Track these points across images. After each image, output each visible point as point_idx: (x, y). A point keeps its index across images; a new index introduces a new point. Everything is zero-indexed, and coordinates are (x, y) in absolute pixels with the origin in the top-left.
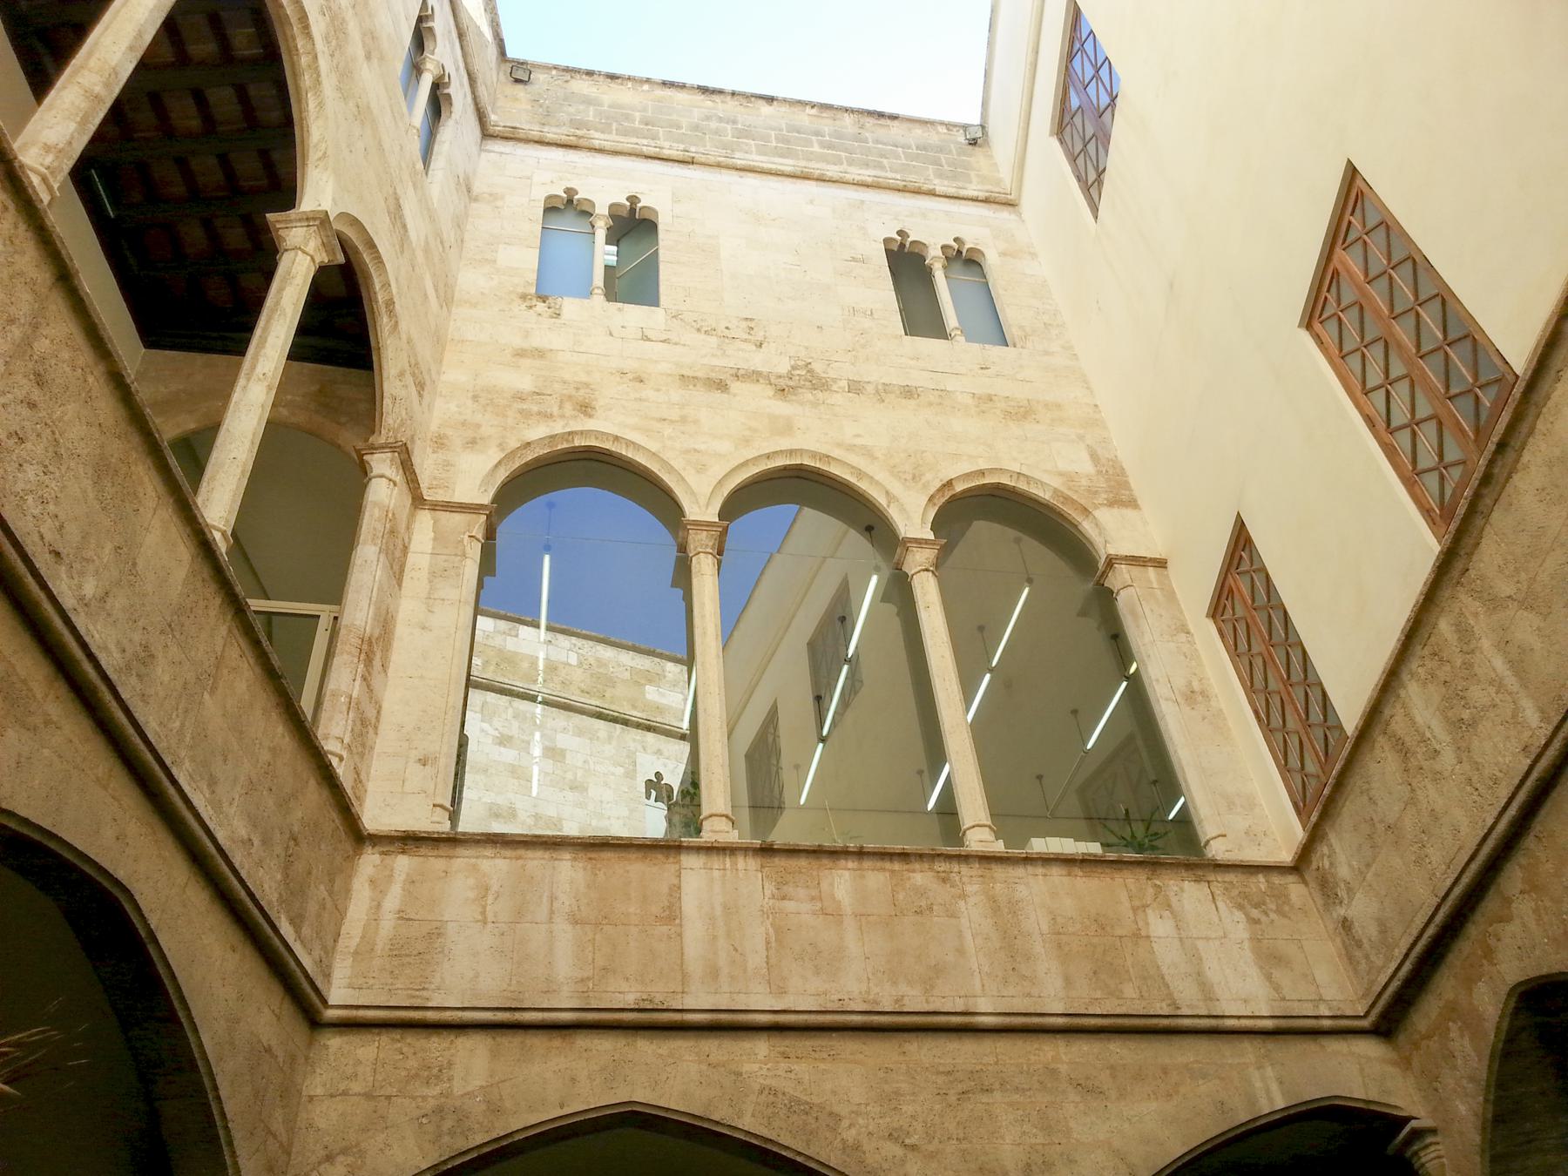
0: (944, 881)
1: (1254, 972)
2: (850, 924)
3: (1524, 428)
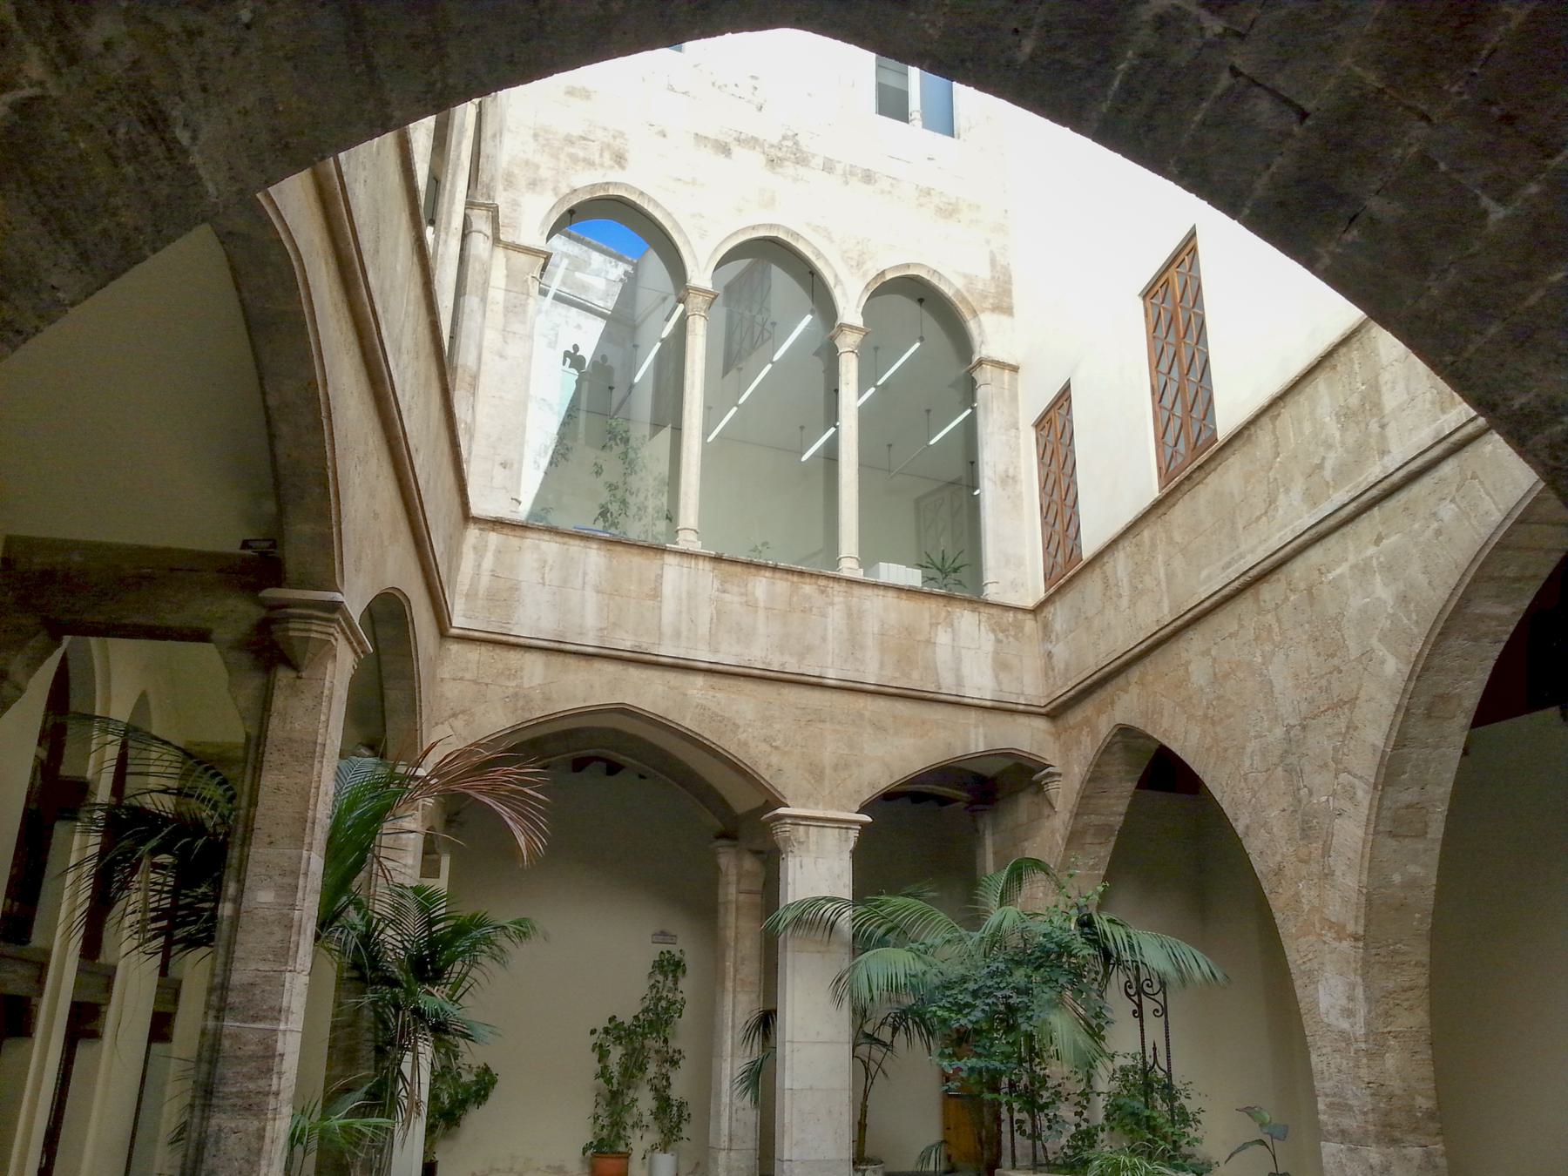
0: (823, 592)
1: (989, 673)
2: (761, 613)
3: (1213, 465)
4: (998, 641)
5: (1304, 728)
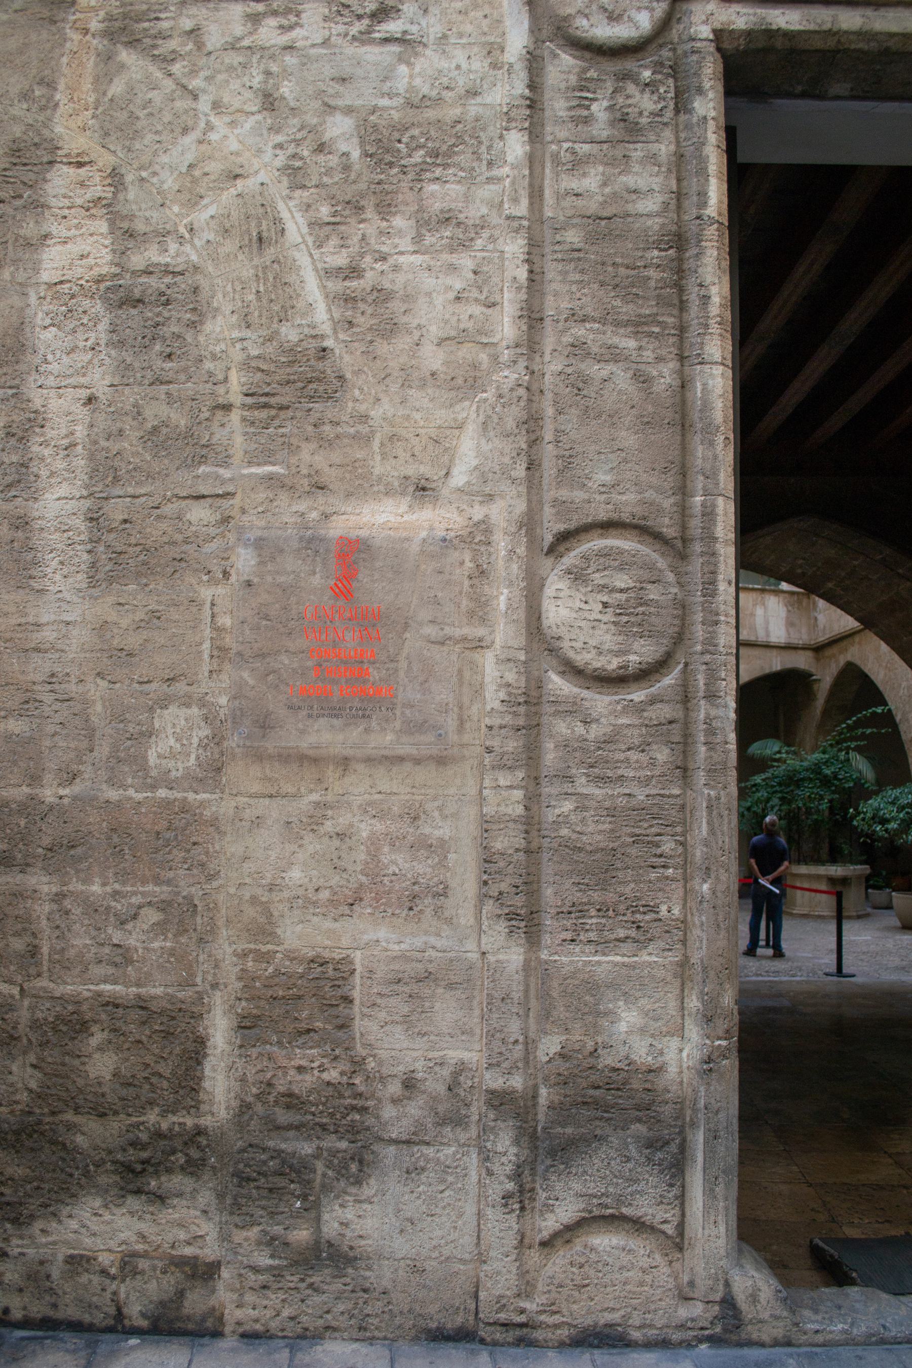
1: (783, 629)
4: (789, 611)
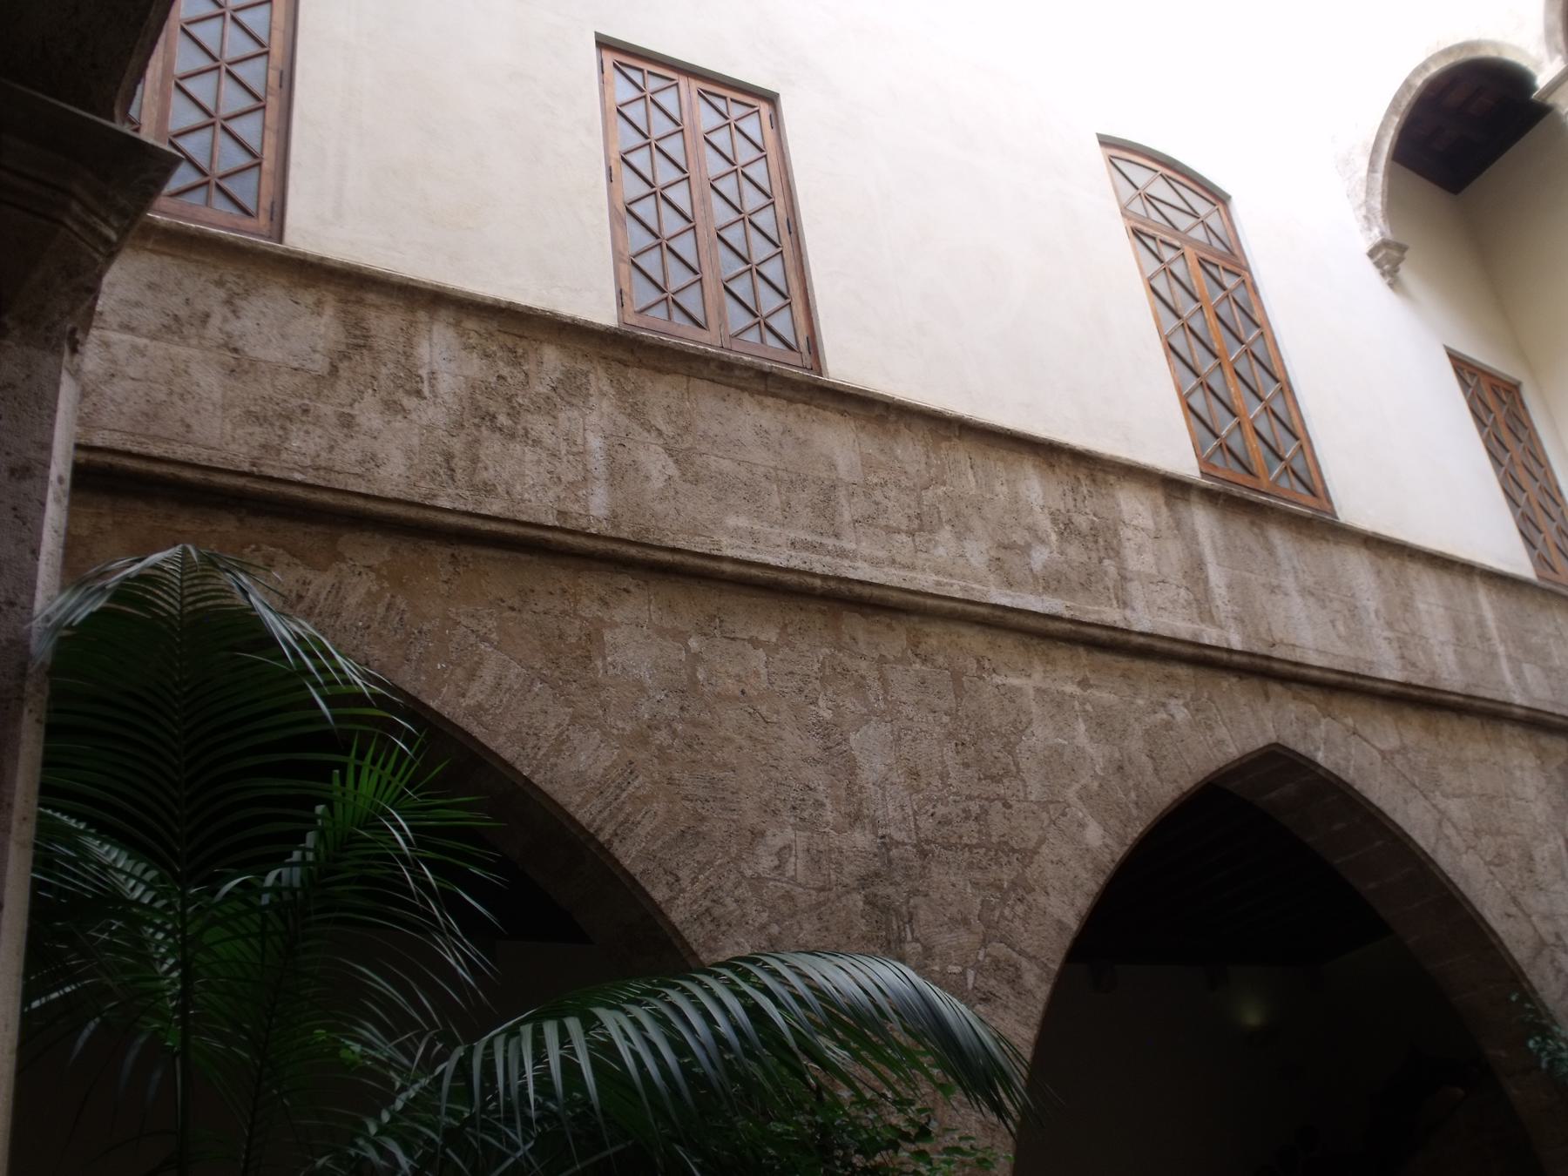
5: (923, 854)
